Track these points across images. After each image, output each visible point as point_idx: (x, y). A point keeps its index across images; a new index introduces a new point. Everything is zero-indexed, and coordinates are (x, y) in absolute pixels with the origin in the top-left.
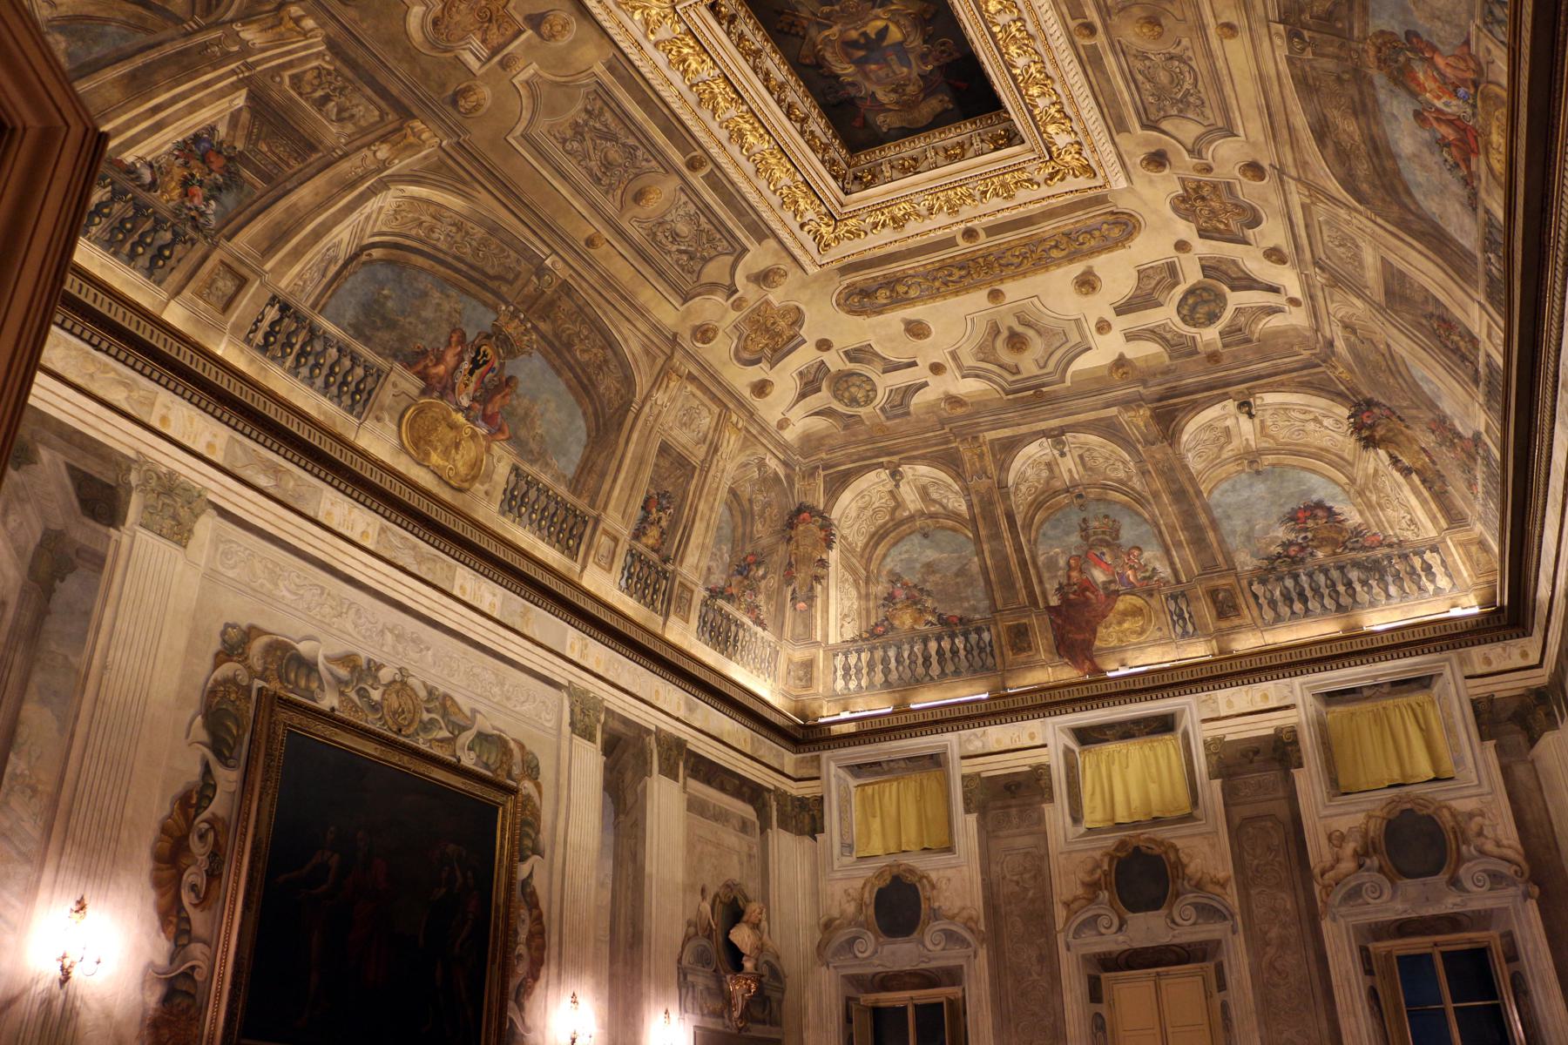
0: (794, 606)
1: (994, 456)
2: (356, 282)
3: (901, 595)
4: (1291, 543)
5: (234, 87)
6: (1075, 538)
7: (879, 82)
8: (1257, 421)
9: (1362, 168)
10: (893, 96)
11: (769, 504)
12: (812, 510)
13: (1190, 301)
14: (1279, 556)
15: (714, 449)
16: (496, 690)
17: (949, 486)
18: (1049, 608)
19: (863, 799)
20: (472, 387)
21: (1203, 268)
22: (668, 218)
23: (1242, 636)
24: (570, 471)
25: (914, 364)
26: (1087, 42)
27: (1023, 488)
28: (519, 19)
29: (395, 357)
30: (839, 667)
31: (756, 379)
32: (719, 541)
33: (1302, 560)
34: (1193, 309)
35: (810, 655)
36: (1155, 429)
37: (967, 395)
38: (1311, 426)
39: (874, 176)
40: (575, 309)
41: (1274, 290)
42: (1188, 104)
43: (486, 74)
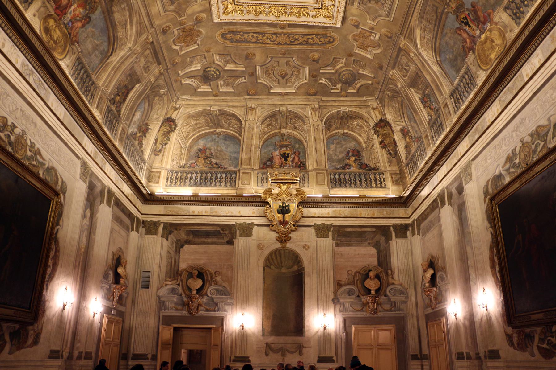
5: (410, 91)
20: (474, 27)
28: (359, 30)
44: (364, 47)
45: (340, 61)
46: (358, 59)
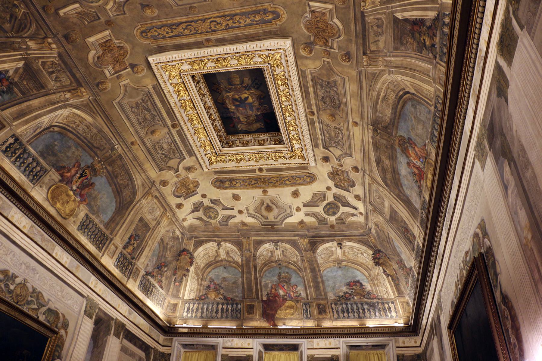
0: (175, 283)
1: (254, 245)
2: (46, 137)
3: (213, 287)
4: (347, 293)
5: (20, 60)
6: (275, 278)
7: (242, 114)
8: (343, 250)
9: (389, 176)
10: (245, 119)
11: (173, 246)
12: (188, 252)
13: (328, 207)
14: (342, 296)
15: (159, 223)
16: (59, 293)
17: (236, 253)
18: (262, 301)
19: (185, 357)
20: (78, 183)
21: (334, 197)
22: (161, 142)
23: (326, 322)
24: (106, 220)
25: (233, 209)
26: (311, 117)
27: (261, 258)
28: (127, 64)
29: (53, 166)
30: (186, 308)
31: (179, 202)
32: (153, 255)
33: (350, 299)
34: (329, 209)
35: (176, 302)
36: (309, 247)
37: (249, 223)
38: (360, 255)
39: (233, 144)
40: (121, 165)
41: (355, 208)
42: (339, 144)
43: (111, 79)
44: (106, 45)
45: (115, 11)
46: (96, 22)
